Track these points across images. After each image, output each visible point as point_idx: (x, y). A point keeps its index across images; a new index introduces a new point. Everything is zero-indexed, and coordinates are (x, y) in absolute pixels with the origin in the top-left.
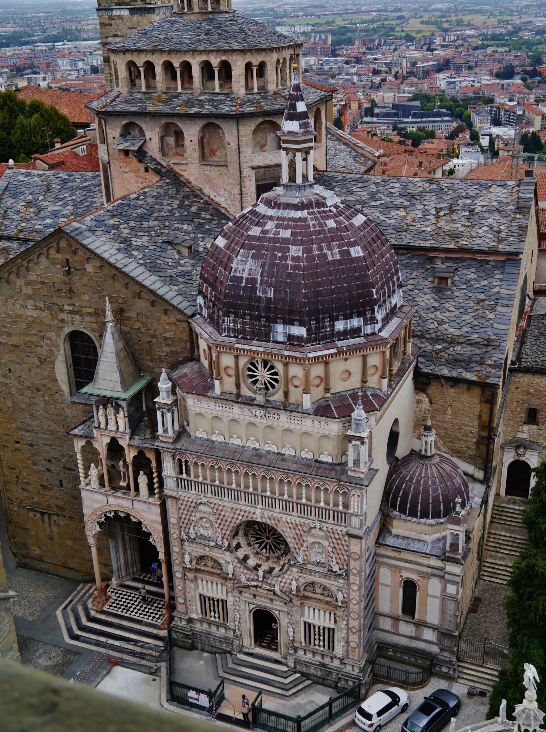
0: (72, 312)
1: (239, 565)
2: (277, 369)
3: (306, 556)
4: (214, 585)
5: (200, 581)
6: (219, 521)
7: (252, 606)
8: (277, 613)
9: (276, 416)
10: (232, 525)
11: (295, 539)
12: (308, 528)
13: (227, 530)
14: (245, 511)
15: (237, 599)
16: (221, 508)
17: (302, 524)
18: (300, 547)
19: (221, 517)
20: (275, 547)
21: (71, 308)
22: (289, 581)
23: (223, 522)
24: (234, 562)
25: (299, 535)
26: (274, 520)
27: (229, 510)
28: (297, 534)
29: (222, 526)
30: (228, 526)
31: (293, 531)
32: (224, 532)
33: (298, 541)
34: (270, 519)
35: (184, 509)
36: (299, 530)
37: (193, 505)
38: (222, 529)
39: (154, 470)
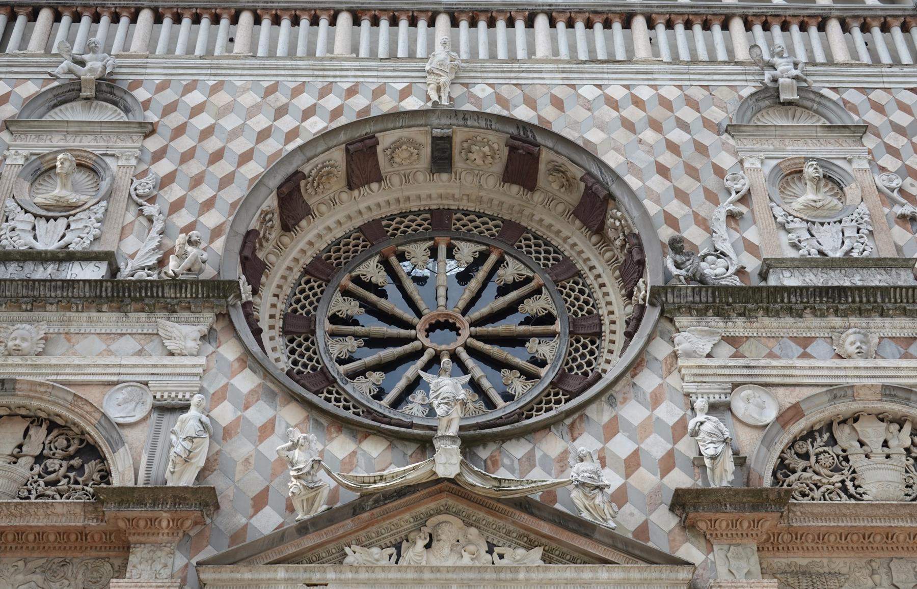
1: (260, 413)
3: (752, 248)
6: (164, 167)
10: (253, 169)
11: (663, 171)
12: (731, 108)
13: (209, 205)
14: (351, 92)
16: (195, 98)
17: (698, 94)
18: (704, 208)
19: (184, 143)
22: (657, 446)
23: (194, 168)
24: (219, 397)
25: (688, 152)
26: (531, 103)
28: (673, 148)
29: (175, 192)
30: (226, 181)
31: (649, 135)
32: (183, 218)
33: (685, 183)
36: (684, 126)
38: (177, 206)
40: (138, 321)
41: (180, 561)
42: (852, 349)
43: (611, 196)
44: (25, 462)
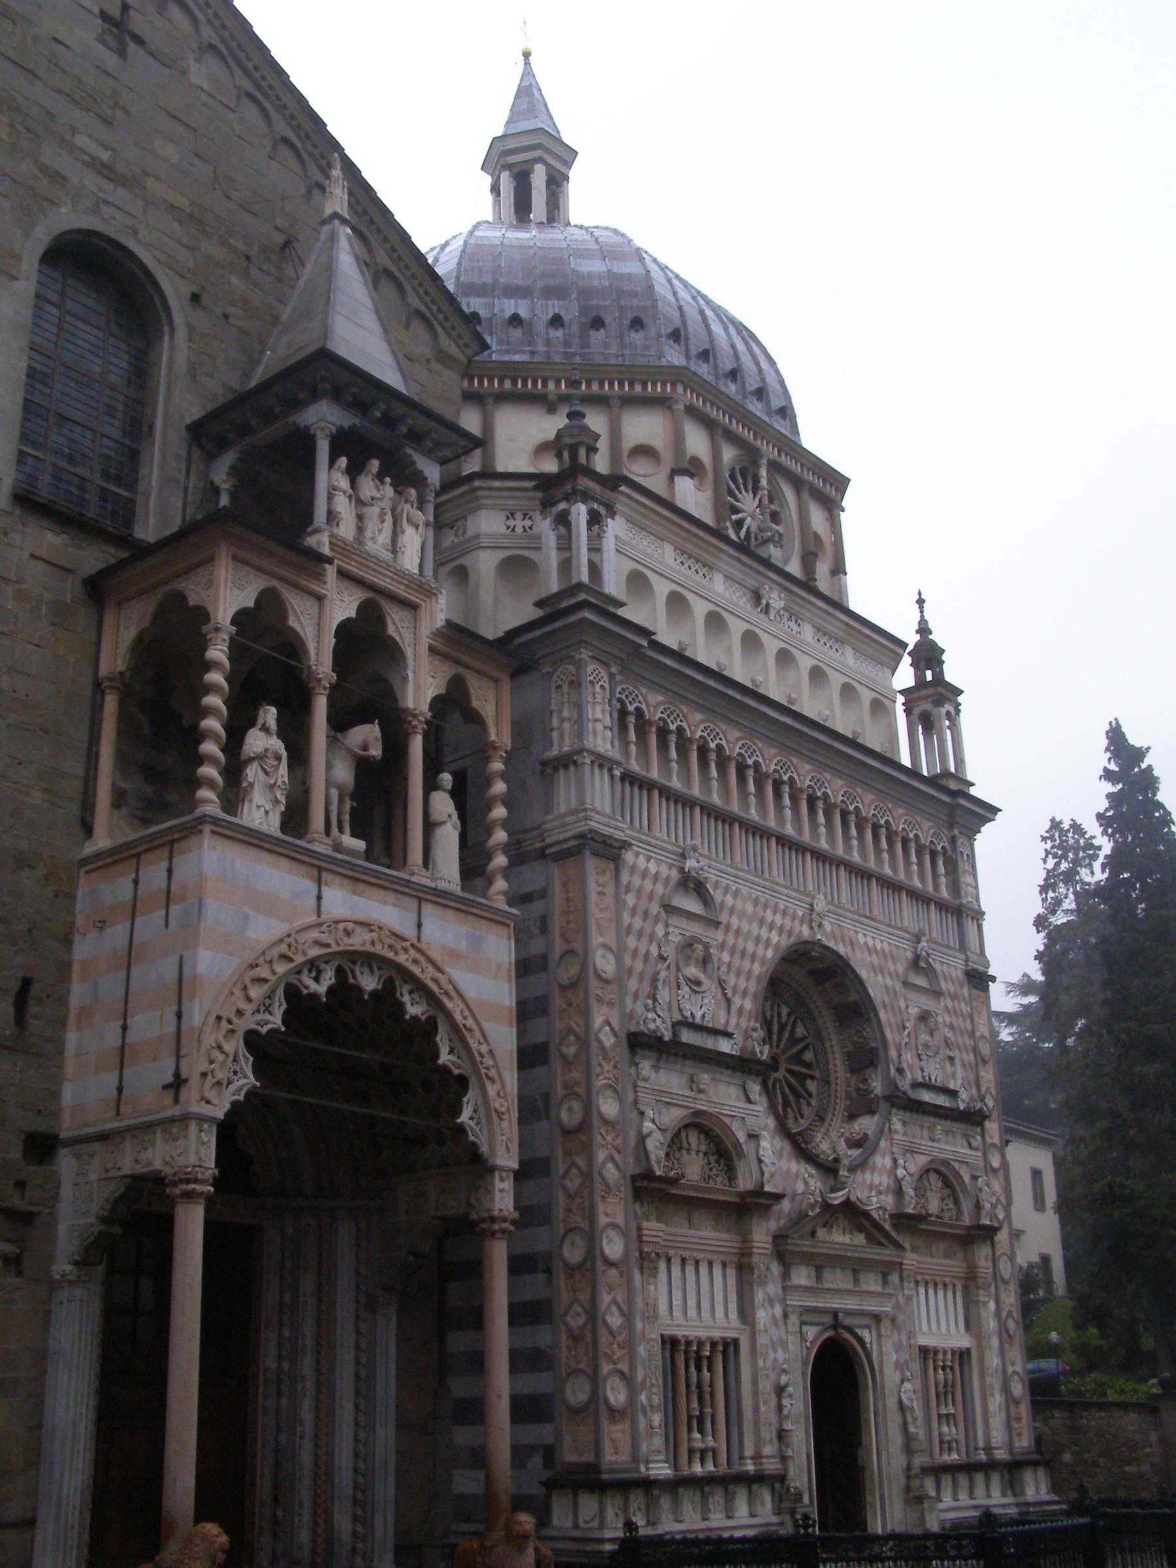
0: (105, 171)
2: (783, 503)
4: (704, 1270)
5: (662, 1266)
7: (811, 1332)
8: (866, 1335)
9: (793, 625)
10: (757, 969)
15: (778, 1311)
20: (797, 1096)
21: (105, 156)
27: (749, 907)
34: (835, 938)
35: (634, 912)
37: (660, 889)
39: (497, 766)
40: (738, 1078)
41: (765, 1225)
42: (937, 1137)
43: (868, 1020)
44: (701, 1155)
